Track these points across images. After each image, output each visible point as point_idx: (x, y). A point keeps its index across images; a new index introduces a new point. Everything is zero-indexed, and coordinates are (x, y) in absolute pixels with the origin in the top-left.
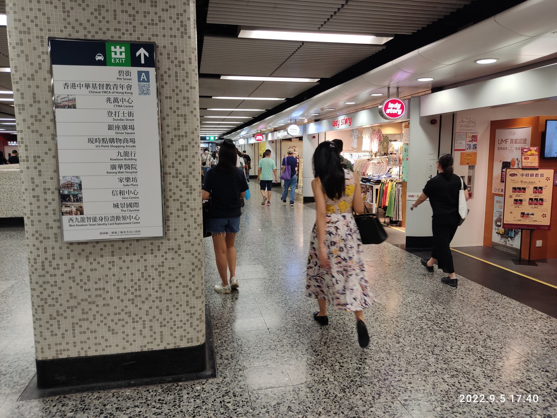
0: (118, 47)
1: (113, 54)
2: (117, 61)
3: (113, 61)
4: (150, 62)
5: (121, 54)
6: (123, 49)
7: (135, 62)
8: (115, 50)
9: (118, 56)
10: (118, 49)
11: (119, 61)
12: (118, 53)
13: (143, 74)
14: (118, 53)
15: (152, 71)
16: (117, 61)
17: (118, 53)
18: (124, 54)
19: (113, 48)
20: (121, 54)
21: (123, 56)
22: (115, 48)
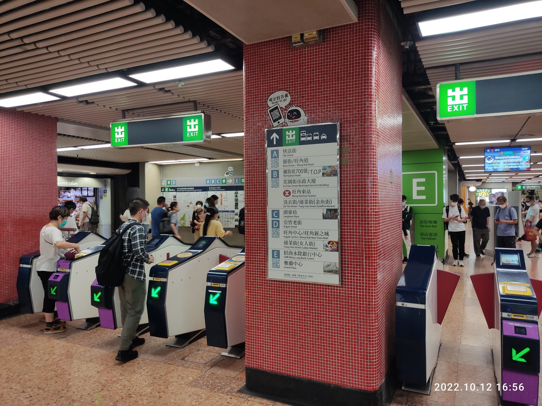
1: (287, 137)
5: (292, 137)
8: (289, 134)
9: (291, 138)
12: (291, 136)
14: (291, 136)
21: (294, 138)
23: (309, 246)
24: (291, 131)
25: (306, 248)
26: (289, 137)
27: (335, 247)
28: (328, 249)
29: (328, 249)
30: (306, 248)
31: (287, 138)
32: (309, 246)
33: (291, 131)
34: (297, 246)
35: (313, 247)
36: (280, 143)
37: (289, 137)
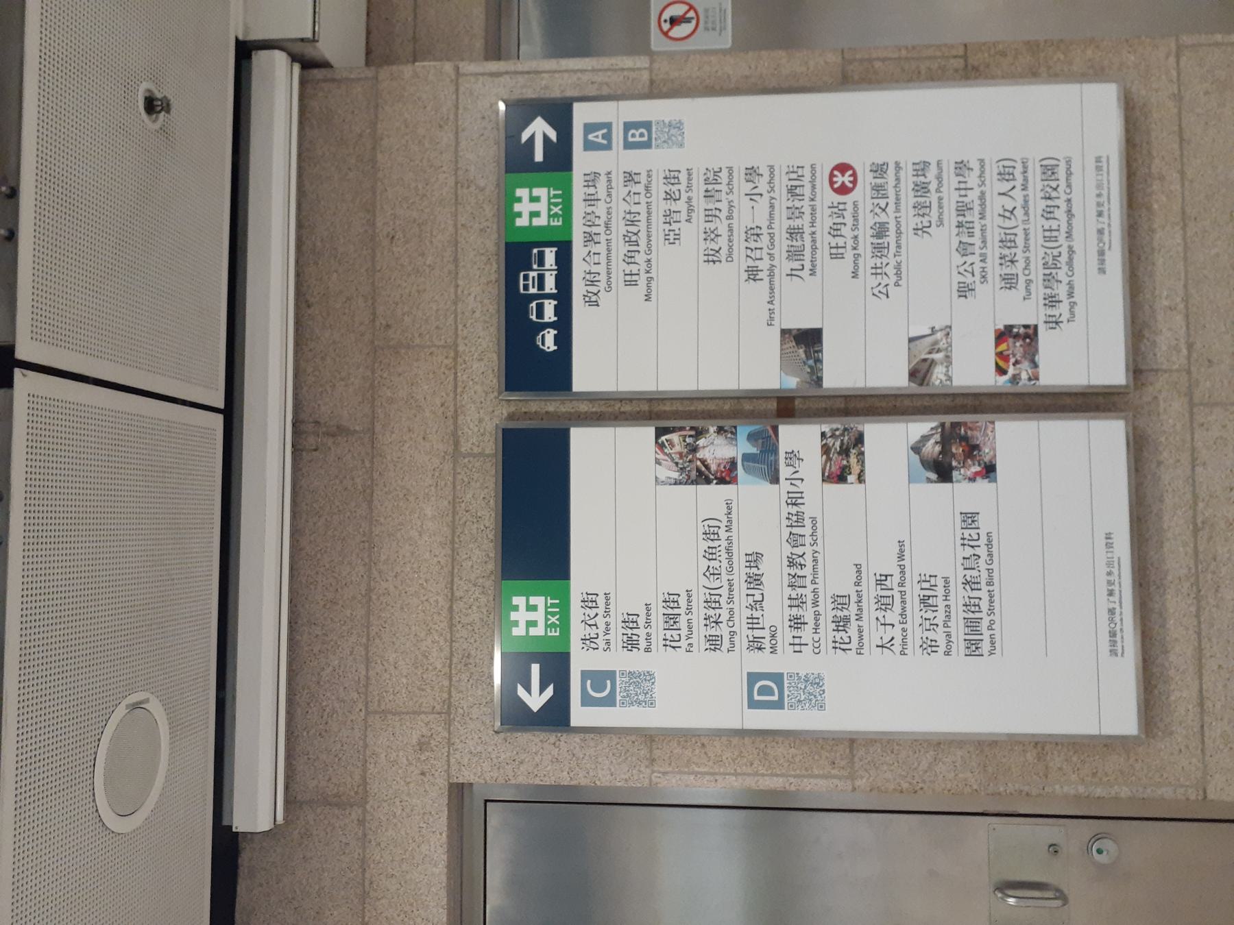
0: (517, 207)
2: (556, 210)
3: (557, 223)
4: (559, 113)
5: (535, 199)
6: (522, 192)
7: (559, 158)
9: (542, 207)
10: (524, 207)
11: (556, 205)
13: (591, 137)
15: (582, 114)
16: (556, 210)
17: (533, 207)
18: (537, 192)
20: (535, 199)
21: (541, 192)
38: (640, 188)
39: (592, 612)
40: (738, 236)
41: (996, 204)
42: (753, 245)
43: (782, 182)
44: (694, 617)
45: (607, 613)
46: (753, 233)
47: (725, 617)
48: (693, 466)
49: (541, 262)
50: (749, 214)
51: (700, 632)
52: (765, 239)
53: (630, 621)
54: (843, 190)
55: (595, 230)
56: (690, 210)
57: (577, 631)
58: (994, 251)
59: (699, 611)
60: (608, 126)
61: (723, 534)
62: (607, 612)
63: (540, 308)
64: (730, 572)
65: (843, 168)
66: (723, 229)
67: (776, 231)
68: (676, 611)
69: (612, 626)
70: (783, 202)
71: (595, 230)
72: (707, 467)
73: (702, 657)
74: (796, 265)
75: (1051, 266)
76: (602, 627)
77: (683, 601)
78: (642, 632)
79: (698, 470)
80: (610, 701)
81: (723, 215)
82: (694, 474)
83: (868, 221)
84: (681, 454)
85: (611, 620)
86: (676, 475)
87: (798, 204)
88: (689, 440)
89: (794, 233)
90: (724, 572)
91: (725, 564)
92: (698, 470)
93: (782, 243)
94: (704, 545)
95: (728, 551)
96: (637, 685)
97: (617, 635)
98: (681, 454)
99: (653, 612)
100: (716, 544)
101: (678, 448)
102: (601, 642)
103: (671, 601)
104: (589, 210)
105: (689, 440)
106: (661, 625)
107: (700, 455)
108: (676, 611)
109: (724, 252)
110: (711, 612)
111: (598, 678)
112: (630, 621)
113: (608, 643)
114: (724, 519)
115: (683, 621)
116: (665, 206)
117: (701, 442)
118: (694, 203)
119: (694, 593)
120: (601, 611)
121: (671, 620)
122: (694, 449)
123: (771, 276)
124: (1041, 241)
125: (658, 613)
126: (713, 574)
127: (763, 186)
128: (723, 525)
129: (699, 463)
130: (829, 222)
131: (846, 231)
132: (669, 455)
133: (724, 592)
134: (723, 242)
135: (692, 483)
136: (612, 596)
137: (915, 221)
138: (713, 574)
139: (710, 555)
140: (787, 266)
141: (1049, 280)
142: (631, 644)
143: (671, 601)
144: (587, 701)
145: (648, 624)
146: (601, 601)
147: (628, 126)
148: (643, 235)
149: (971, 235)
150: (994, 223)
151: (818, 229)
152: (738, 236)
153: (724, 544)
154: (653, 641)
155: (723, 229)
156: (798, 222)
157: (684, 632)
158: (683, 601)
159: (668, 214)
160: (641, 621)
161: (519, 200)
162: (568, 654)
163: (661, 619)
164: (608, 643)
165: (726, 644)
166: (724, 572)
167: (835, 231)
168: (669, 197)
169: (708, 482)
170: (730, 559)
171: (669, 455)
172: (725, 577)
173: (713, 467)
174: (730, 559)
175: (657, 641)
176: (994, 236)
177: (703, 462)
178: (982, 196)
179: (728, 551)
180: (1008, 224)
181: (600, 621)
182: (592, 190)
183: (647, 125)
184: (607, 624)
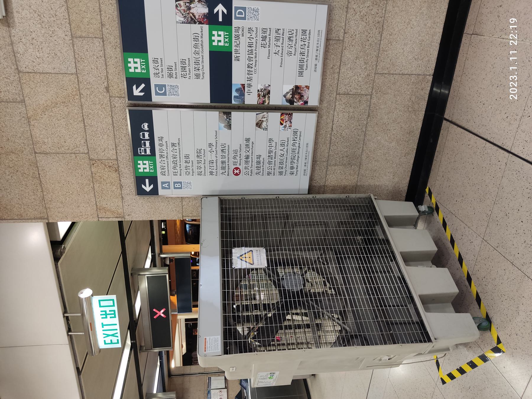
5: (145, 164)
19: (140, 171)
20: (145, 164)
22: (140, 168)
23: (286, 147)
24: (139, 166)
25: (287, 151)
26: (146, 168)
27: (286, 117)
28: (288, 126)
29: (288, 126)
30: (287, 151)
31: (147, 170)
32: (286, 147)
33: (139, 166)
34: (285, 160)
35: (286, 143)
36: (154, 180)
37: (146, 168)
38: (177, 148)
39: (157, 65)
40: (207, 163)
41: (279, 153)
42: (211, 165)
43: (219, 148)
44: (191, 67)
45: (162, 65)
46: (211, 162)
47: (201, 68)
48: (189, 16)
49: (145, 145)
50: (210, 157)
51: (193, 72)
52: (215, 163)
53: (170, 68)
54: (237, 168)
55: (163, 154)
56: (193, 172)
57: (152, 71)
58: (278, 165)
59: (193, 66)
60: (169, 182)
61: (200, 39)
62: (162, 65)
63: (144, 135)
64: (202, 52)
65: (237, 175)
66: (202, 166)
67: (218, 150)
68: (185, 65)
69: (164, 70)
70: (220, 153)
71: (163, 154)
72: (194, 16)
73: (194, 80)
74: (224, 171)
75: (293, 158)
76: (160, 70)
77: (187, 62)
78: (174, 72)
79: (191, 18)
80: (165, 94)
81: (203, 162)
82: (190, 19)
83: (244, 154)
84: (184, 10)
85: (163, 68)
86: (182, 19)
87: (224, 154)
88: (187, 4)
89: (223, 162)
90: (200, 52)
91: (201, 50)
92: (191, 18)
93: (220, 165)
94: (194, 43)
95: (202, 45)
96: (173, 89)
97: (166, 72)
98: (184, 10)
99: (177, 65)
100: (197, 42)
101: (183, 8)
102: (160, 75)
103: (183, 62)
104: (161, 148)
105: (187, 4)
106: (180, 70)
107: (192, 11)
108: (185, 65)
109: (203, 172)
110: (196, 66)
111: (161, 87)
112: (170, 68)
113: (163, 75)
114: (200, 34)
115: (187, 69)
116: (185, 165)
117: (192, 6)
118: (194, 170)
119: (191, 59)
120: (160, 64)
121: (184, 68)
122: (189, 8)
123: (217, 162)
124: (291, 152)
125: (179, 65)
126: (197, 53)
127: (214, 148)
128: (200, 36)
129: (191, 15)
130: (233, 155)
131: (237, 158)
132: (179, 10)
133: (201, 59)
134: (203, 170)
135: (189, 23)
136: (163, 59)
137: (256, 171)
138: (197, 53)
139: (196, 46)
140: (221, 171)
141: (292, 162)
142: (170, 76)
143: (183, 62)
144: (157, 94)
145: (176, 69)
146: (159, 61)
147: (175, 183)
148: (178, 161)
149: (272, 159)
150: (278, 157)
151: (230, 156)
152: (207, 163)
153: (200, 42)
154: (178, 75)
155: (202, 166)
156: (224, 160)
157: (188, 72)
158: (187, 62)
159: (186, 167)
160: (174, 68)
161: (140, 164)
162: (149, 79)
163: (180, 68)
164: (163, 75)
165: (201, 77)
166: (200, 52)
167: (235, 158)
168: (186, 162)
169: (195, 23)
170: (202, 48)
171: (179, 10)
172: (201, 54)
173: (197, 17)
174: (202, 48)
175: (179, 75)
176: (278, 160)
177: (193, 14)
178: (275, 153)
179: (202, 45)
180: (282, 158)
181: (159, 68)
182: (161, 142)
183: (181, 183)
184: (162, 69)
